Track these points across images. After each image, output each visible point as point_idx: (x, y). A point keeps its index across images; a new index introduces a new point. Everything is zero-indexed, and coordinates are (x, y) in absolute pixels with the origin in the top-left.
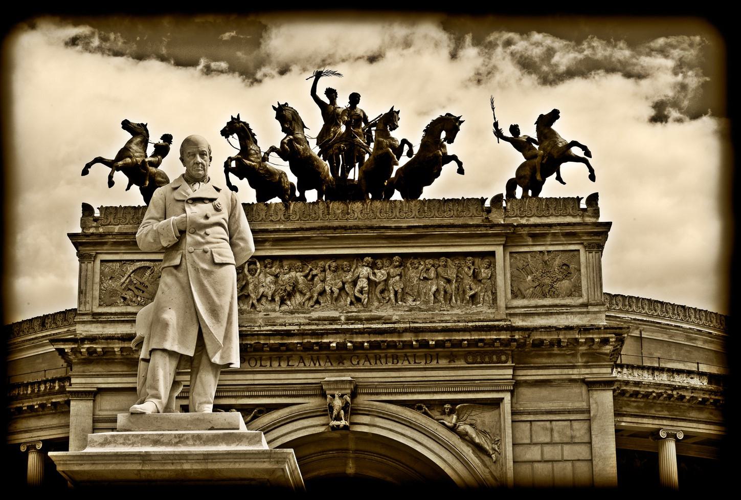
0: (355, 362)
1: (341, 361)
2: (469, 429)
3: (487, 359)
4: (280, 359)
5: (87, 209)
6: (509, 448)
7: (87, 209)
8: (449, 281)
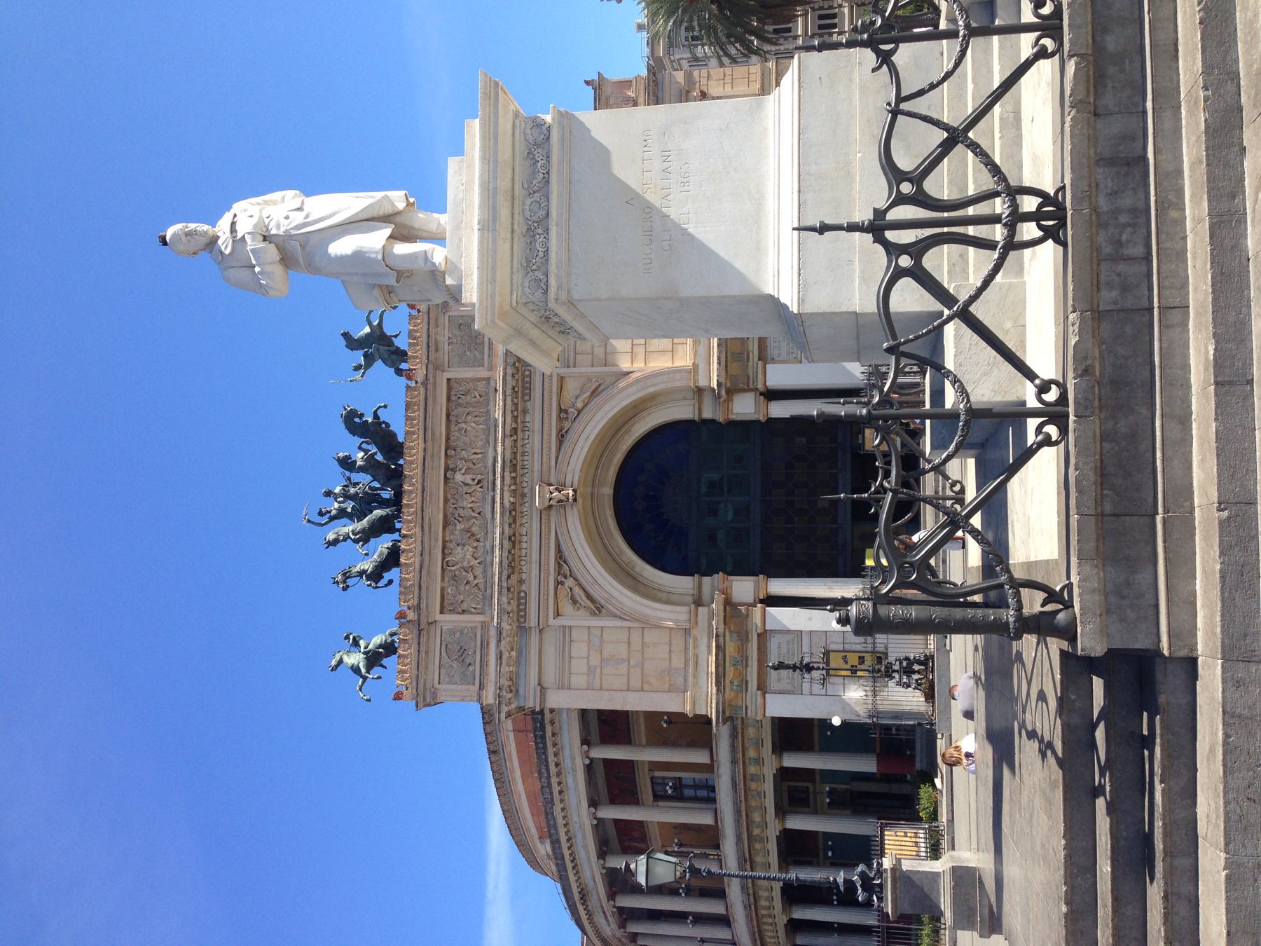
0: (525, 484)
1: (523, 495)
2: (580, 400)
3: (528, 385)
4: (520, 542)
5: (398, 697)
6: (594, 369)
7: (398, 697)
8: (468, 414)
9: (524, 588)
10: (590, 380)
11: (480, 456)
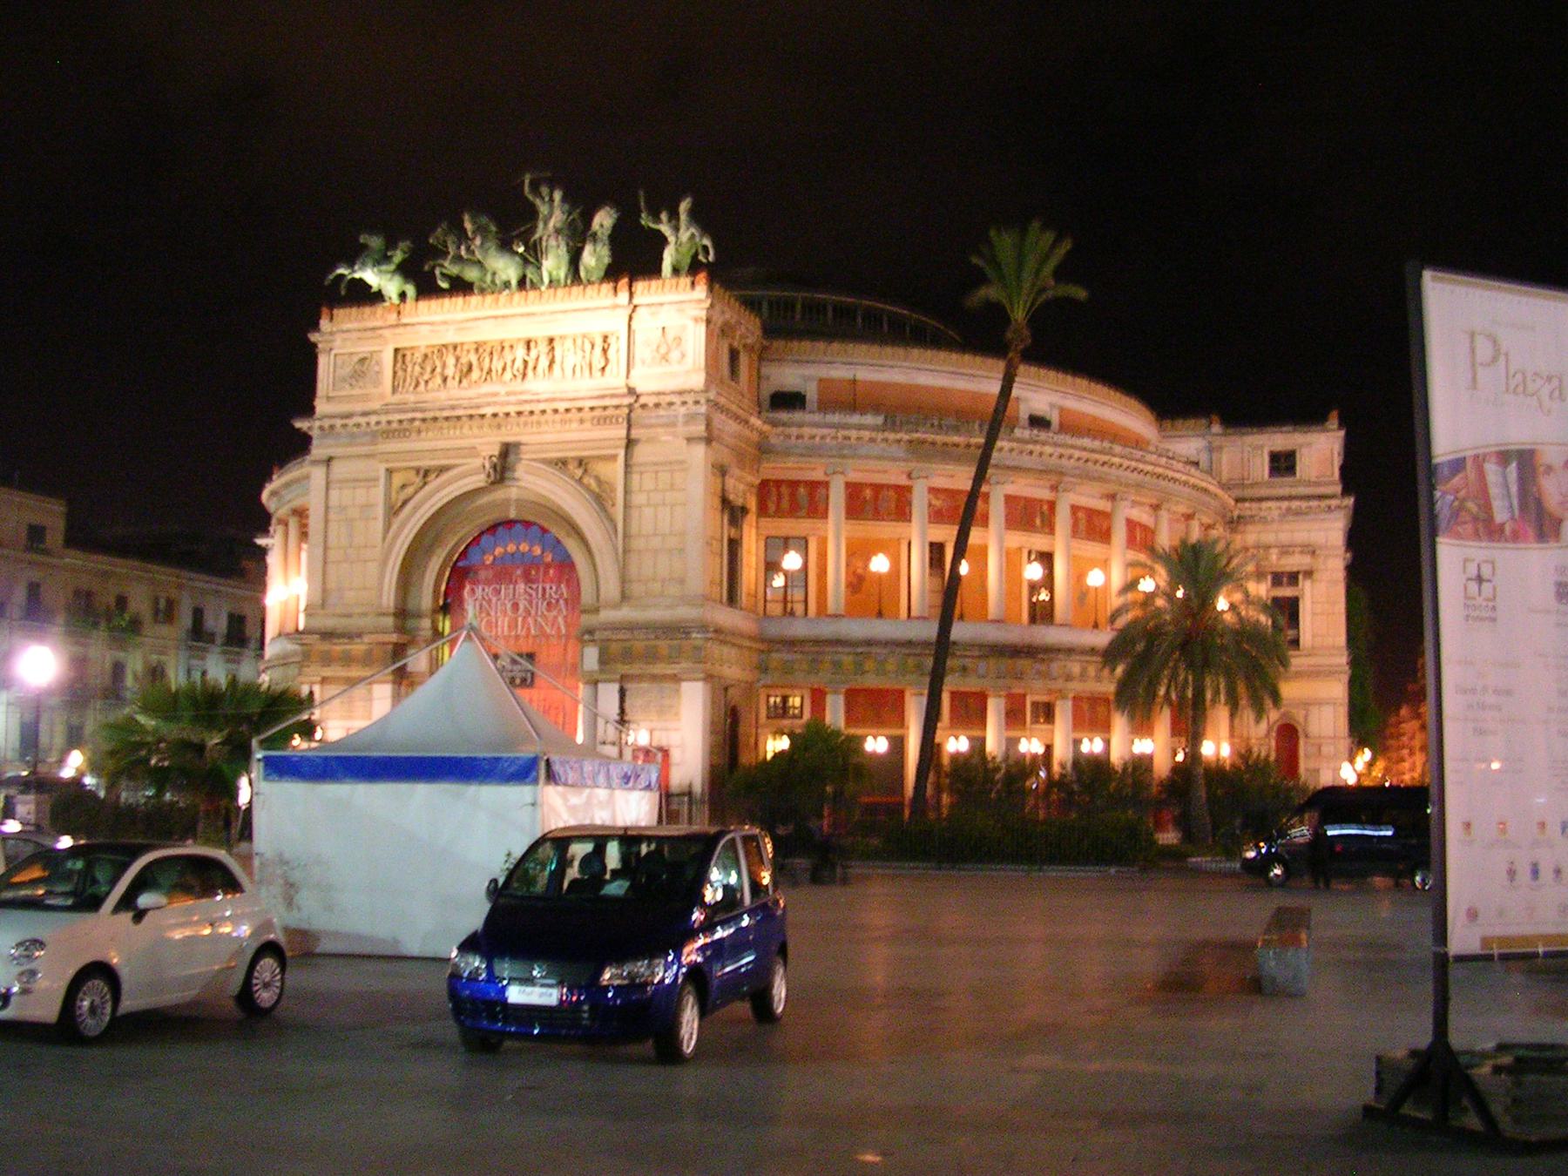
0: (509, 428)
4: (455, 428)
9: (413, 434)
10: (613, 490)
11: (541, 375)
